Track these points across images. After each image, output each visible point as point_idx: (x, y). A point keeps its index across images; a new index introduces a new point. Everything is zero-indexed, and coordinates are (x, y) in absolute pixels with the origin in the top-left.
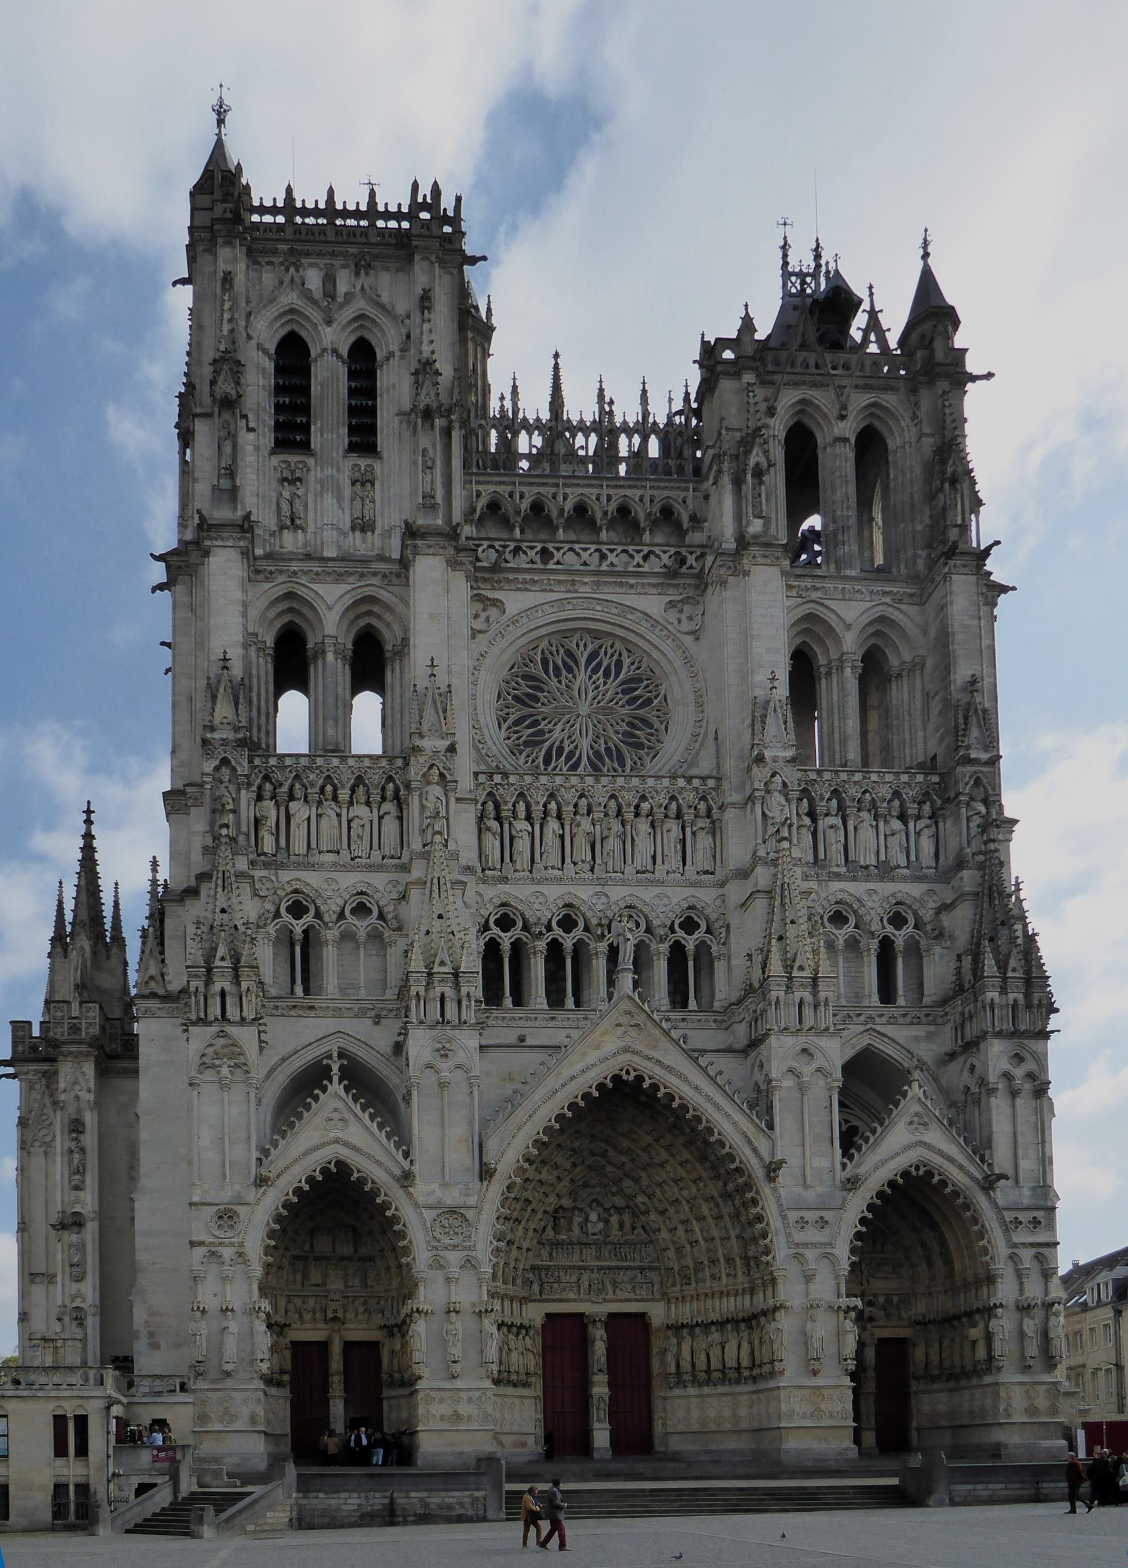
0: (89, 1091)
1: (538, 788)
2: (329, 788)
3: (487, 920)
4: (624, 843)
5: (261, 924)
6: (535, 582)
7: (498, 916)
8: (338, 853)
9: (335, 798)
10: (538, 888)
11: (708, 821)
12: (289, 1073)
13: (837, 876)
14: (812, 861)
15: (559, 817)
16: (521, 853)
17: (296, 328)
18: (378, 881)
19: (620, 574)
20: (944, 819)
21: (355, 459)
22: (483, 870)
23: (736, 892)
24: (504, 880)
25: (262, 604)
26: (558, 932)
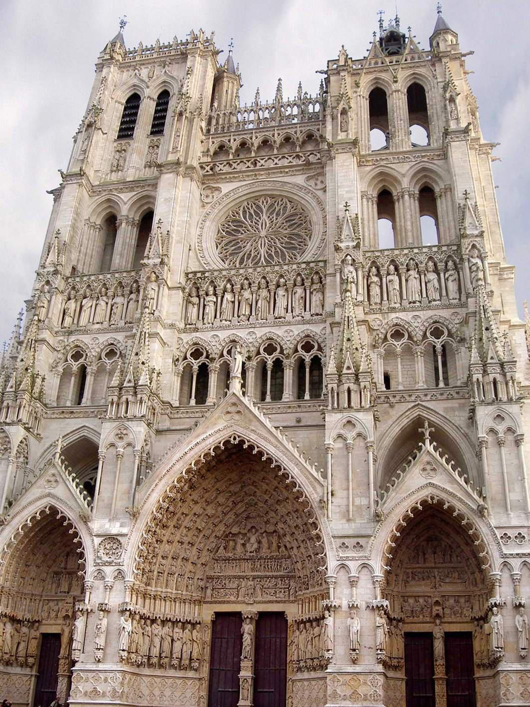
1: (221, 278)
3: (186, 353)
4: (269, 302)
6: (236, 177)
8: (102, 323)
9: (106, 294)
11: (319, 284)
13: (393, 310)
16: (208, 314)
17: (136, 91)
18: (120, 337)
19: (280, 168)
20: (462, 269)
21: (152, 137)
22: (186, 325)
24: (196, 330)
25: (94, 206)
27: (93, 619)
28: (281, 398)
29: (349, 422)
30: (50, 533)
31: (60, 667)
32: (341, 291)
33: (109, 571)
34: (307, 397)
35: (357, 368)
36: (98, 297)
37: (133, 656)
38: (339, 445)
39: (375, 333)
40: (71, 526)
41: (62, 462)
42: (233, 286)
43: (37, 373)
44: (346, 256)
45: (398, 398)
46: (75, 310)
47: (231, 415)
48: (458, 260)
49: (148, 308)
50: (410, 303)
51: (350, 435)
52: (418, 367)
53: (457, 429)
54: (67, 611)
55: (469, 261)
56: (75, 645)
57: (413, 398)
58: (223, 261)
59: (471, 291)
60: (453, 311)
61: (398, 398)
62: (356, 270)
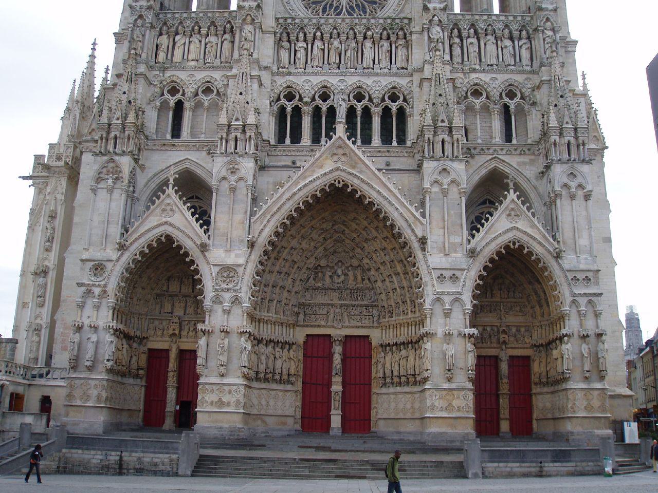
0: (62, 194)
1: (311, 25)
2: (196, 28)
4: (357, 53)
5: (152, 99)
7: (286, 92)
9: (199, 32)
10: (307, 78)
11: (404, 40)
12: (157, 183)
13: (474, 70)
14: (461, 62)
15: (322, 39)
16: (299, 59)
18: (217, 75)
23: (416, 78)
24: (289, 74)
26: (319, 101)
27: (217, 340)
28: (370, 143)
29: (444, 170)
30: (156, 259)
31: (170, 379)
32: (429, 49)
33: (227, 296)
34: (395, 143)
35: (451, 123)
36: (192, 35)
37: (250, 371)
38: (436, 189)
39: (457, 90)
40: (186, 254)
41: (176, 192)
42: (322, 34)
43: (140, 106)
44: (433, 17)
45: (478, 150)
46: (168, 46)
47: (337, 156)
48: (531, 31)
49: (247, 49)
50: (488, 65)
51: (446, 181)
52: (495, 126)
53: (528, 182)
54: (174, 330)
55: (543, 32)
56: (199, 361)
57: (491, 151)
58: (306, 8)
59: (545, 60)
60: (526, 76)
61: (478, 150)
62: (443, 30)
